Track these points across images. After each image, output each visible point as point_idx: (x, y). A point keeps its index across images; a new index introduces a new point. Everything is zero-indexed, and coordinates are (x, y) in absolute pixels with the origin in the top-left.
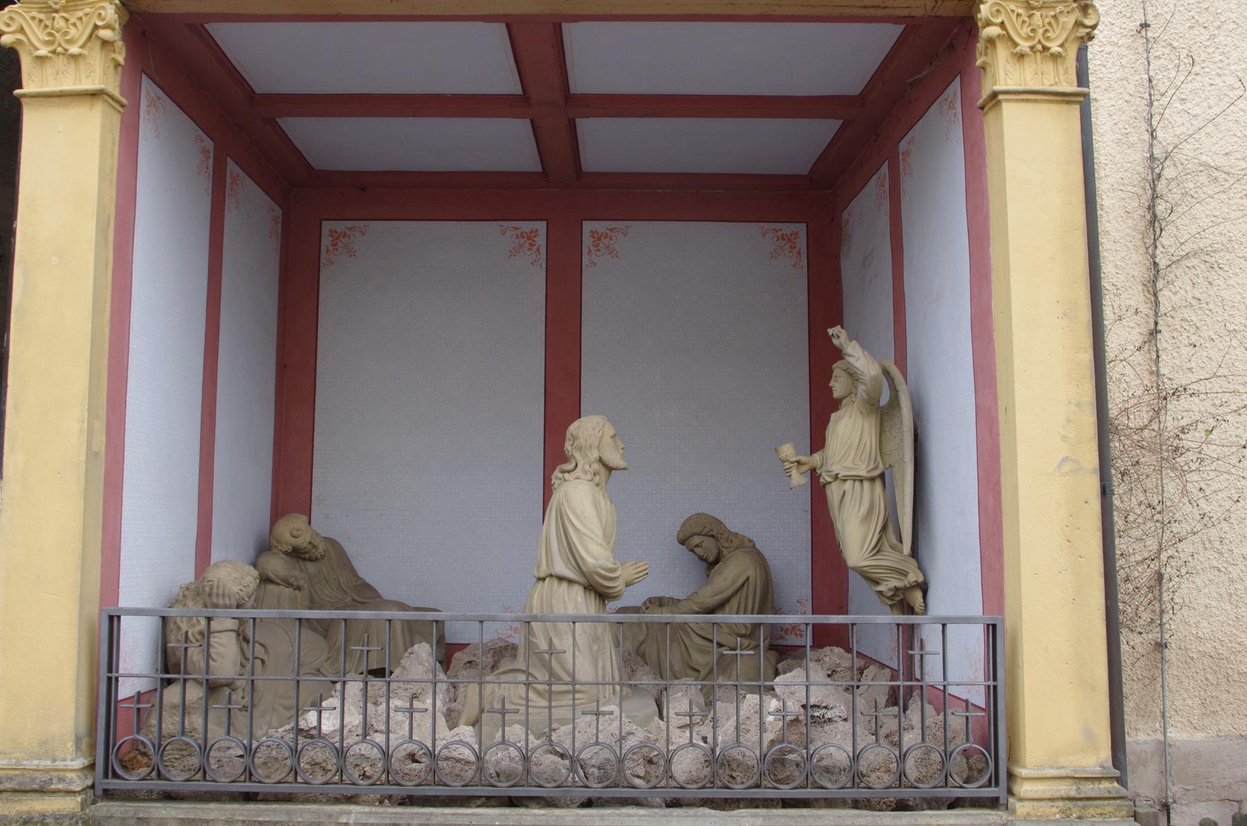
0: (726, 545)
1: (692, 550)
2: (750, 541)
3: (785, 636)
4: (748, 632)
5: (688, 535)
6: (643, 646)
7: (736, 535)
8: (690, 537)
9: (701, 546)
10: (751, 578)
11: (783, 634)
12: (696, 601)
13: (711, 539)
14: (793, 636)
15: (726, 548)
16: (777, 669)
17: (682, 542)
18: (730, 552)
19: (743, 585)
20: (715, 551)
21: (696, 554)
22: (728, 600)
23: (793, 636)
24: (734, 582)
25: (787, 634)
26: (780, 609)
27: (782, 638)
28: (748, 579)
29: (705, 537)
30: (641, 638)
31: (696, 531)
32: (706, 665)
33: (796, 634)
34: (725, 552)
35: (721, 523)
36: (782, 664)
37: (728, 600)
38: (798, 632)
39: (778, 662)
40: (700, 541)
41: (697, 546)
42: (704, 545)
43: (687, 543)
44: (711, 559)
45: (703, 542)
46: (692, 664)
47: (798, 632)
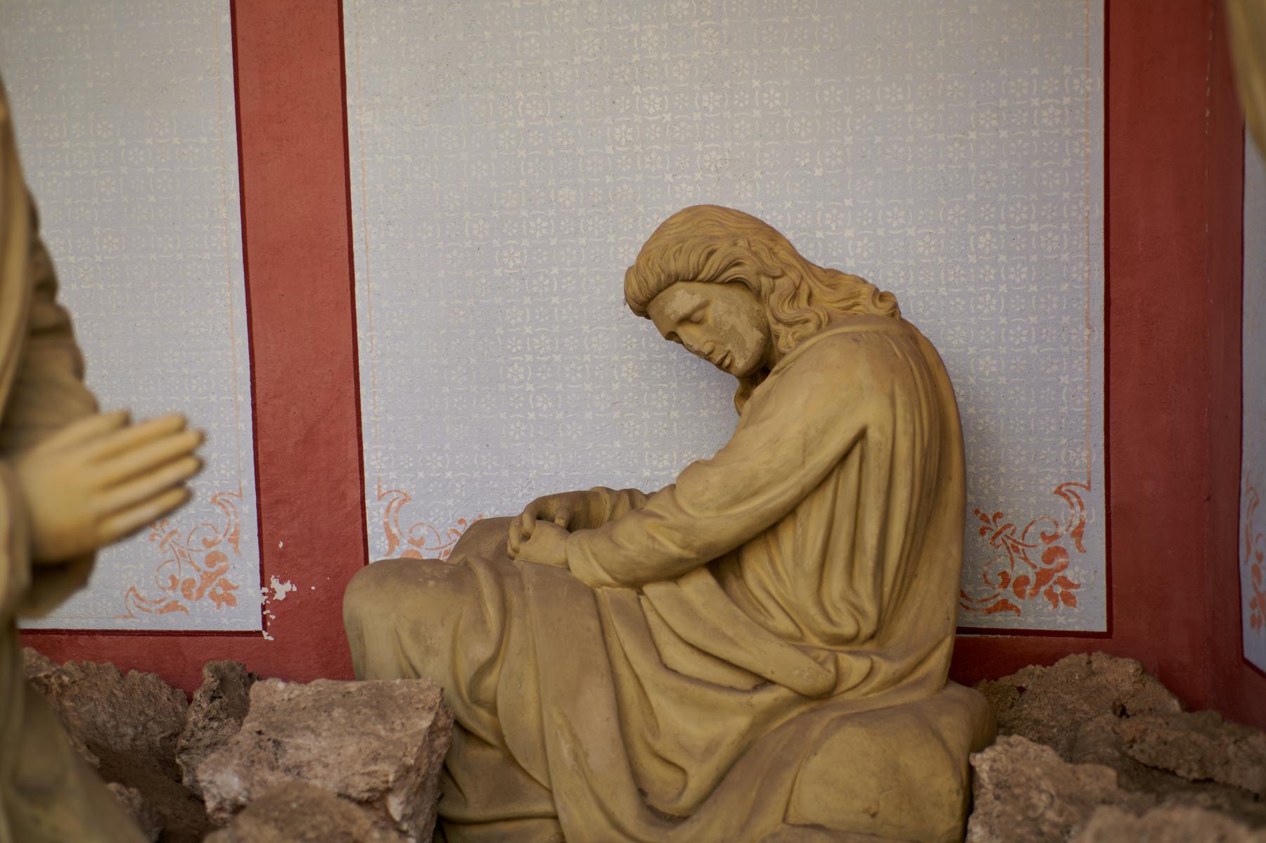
0: (787, 312)
1: (672, 336)
2: (880, 296)
3: (1014, 600)
4: (867, 629)
5: (652, 282)
6: (490, 680)
7: (833, 277)
8: (660, 291)
9: (699, 322)
10: (873, 435)
11: (1009, 593)
12: (671, 519)
13: (735, 294)
14: (1042, 599)
15: (789, 325)
16: (971, 770)
17: (642, 307)
18: (802, 339)
19: (844, 458)
20: (753, 339)
21: (689, 348)
22: (790, 512)
23: (1042, 599)
24: (806, 450)
25: (1020, 594)
26: (998, 515)
27: (1004, 606)
28: (862, 435)
29: (715, 290)
30: (481, 651)
31: (676, 266)
32: (709, 750)
33: (1051, 595)
34: (785, 339)
35: (774, 235)
36: (989, 753)
37: (790, 512)
38: (1059, 590)
39: (978, 746)
40: (696, 301)
41: (686, 320)
42: (710, 314)
43: (652, 311)
44: (741, 364)
45: (704, 306)
46: (659, 746)
47: (1059, 590)
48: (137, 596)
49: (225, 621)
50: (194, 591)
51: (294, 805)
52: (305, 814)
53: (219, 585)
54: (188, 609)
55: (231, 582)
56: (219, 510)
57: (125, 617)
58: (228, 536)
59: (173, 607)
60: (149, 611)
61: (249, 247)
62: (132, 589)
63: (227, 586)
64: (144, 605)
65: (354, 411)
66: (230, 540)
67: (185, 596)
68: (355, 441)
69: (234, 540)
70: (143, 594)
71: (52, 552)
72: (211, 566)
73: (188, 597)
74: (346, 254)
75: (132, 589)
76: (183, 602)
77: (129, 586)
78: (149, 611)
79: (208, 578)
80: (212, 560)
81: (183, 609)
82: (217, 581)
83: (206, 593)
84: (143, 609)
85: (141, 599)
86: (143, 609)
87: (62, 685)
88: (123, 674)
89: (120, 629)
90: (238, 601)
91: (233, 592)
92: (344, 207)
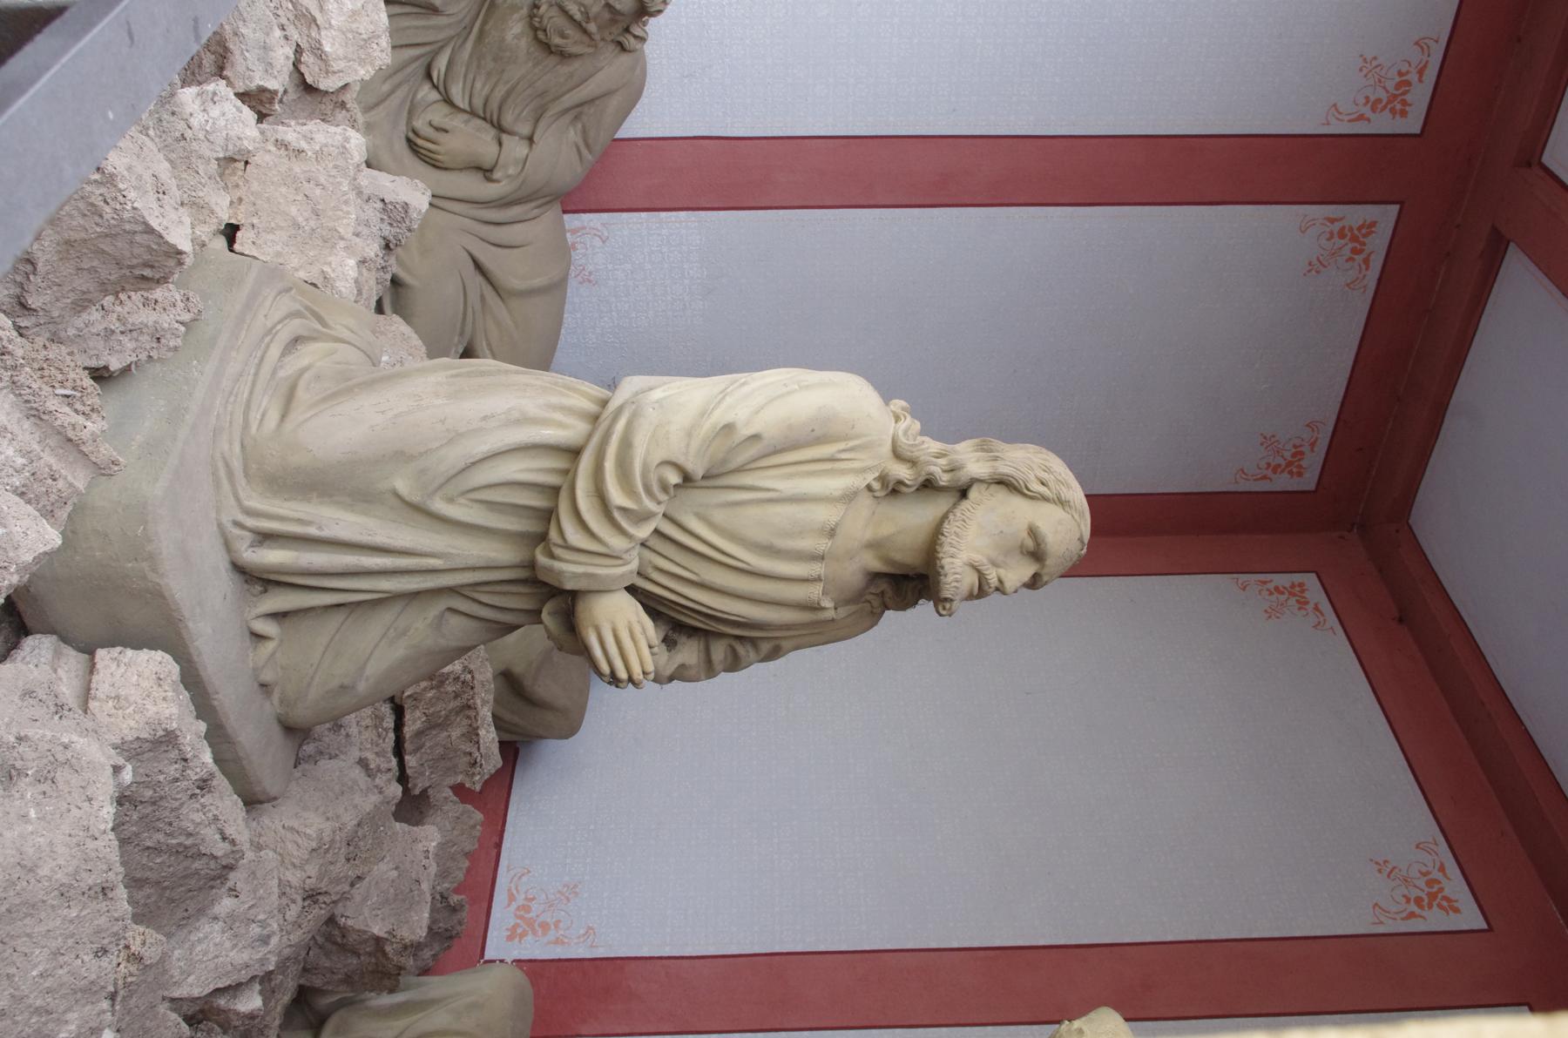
48: (523, 875)
49: (495, 934)
50: (522, 913)
51: (382, 828)
52: (374, 832)
53: (524, 931)
54: (508, 909)
55: (525, 938)
56: (582, 932)
57: (508, 867)
58: (561, 937)
59: (512, 898)
60: (511, 882)
61: (783, 957)
62: (529, 872)
63: (522, 936)
64: (516, 879)
65: (652, 1030)
66: (558, 938)
67: (519, 907)
68: (627, 1031)
69: (557, 942)
70: (524, 879)
71: (581, 607)
72: (539, 925)
73: (518, 909)
74: (778, 1027)
75: (529, 872)
76: (514, 906)
77: (531, 870)
78: (511, 882)
79: (530, 923)
80: (545, 927)
81: (509, 905)
82: (527, 929)
83: (519, 921)
84: (512, 878)
85: (520, 877)
86: (512, 878)
87: (474, 774)
88: (467, 855)
89: (500, 863)
90: (510, 943)
91: (517, 939)
92: (814, 1025)
